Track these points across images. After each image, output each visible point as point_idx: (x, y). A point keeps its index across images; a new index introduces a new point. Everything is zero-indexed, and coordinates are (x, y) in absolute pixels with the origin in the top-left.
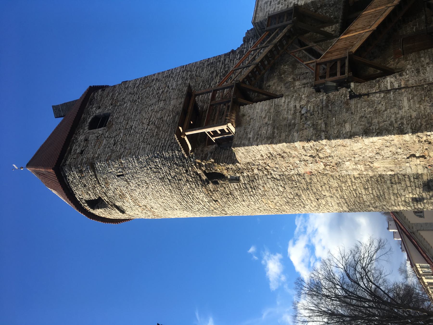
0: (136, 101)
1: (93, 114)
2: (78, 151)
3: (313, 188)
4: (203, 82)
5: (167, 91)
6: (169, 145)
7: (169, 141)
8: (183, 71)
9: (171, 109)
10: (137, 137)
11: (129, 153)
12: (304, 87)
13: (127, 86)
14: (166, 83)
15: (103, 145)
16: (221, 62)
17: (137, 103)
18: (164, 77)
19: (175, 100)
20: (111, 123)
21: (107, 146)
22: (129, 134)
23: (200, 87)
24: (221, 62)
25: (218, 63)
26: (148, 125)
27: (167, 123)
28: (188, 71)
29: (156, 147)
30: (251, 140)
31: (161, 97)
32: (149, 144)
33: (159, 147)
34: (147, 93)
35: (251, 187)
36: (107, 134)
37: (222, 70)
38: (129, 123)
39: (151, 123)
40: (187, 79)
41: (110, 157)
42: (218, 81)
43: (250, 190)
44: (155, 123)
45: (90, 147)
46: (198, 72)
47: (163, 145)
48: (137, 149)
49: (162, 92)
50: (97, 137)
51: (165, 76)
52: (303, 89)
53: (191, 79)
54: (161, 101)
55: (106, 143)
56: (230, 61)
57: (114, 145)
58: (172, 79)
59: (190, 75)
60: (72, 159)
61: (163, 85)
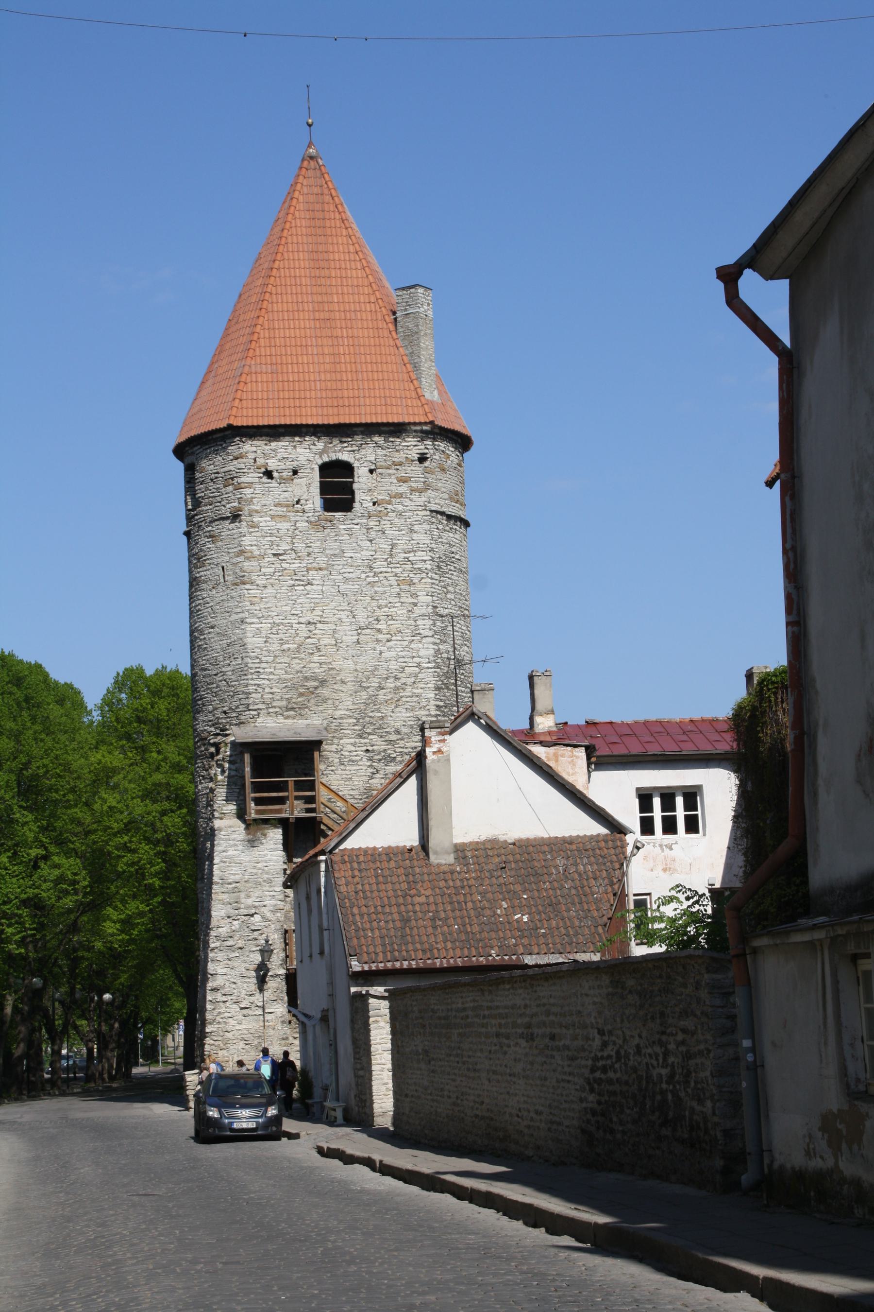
4: (383, 717)
5: (378, 641)
6: (259, 685)
7: (267, 682)
8: (418, 665)
10: (284, 608)
11: (254, 599)
13: (416, 528)
14: (400, 632)
17: (363, 575)
18: (415, 621)
19: (353, 667)
22: (294, 585)
23: (371, 714)
27: (304, 667)
28: (416, 676)
29: (258, 658)
32: (265, 642)
34: (385, 592)
39: (312, 627)
40: (396, 678)
41: (248, 558)
42: (375, 748)
44: (309, 637)
45: (277, 492)
46: (408, 699)
47: (261, 670)
48: (260, 615)
49: (379, 631)
50: (298, 502)
53: (397, 689)
61: (396, 625)
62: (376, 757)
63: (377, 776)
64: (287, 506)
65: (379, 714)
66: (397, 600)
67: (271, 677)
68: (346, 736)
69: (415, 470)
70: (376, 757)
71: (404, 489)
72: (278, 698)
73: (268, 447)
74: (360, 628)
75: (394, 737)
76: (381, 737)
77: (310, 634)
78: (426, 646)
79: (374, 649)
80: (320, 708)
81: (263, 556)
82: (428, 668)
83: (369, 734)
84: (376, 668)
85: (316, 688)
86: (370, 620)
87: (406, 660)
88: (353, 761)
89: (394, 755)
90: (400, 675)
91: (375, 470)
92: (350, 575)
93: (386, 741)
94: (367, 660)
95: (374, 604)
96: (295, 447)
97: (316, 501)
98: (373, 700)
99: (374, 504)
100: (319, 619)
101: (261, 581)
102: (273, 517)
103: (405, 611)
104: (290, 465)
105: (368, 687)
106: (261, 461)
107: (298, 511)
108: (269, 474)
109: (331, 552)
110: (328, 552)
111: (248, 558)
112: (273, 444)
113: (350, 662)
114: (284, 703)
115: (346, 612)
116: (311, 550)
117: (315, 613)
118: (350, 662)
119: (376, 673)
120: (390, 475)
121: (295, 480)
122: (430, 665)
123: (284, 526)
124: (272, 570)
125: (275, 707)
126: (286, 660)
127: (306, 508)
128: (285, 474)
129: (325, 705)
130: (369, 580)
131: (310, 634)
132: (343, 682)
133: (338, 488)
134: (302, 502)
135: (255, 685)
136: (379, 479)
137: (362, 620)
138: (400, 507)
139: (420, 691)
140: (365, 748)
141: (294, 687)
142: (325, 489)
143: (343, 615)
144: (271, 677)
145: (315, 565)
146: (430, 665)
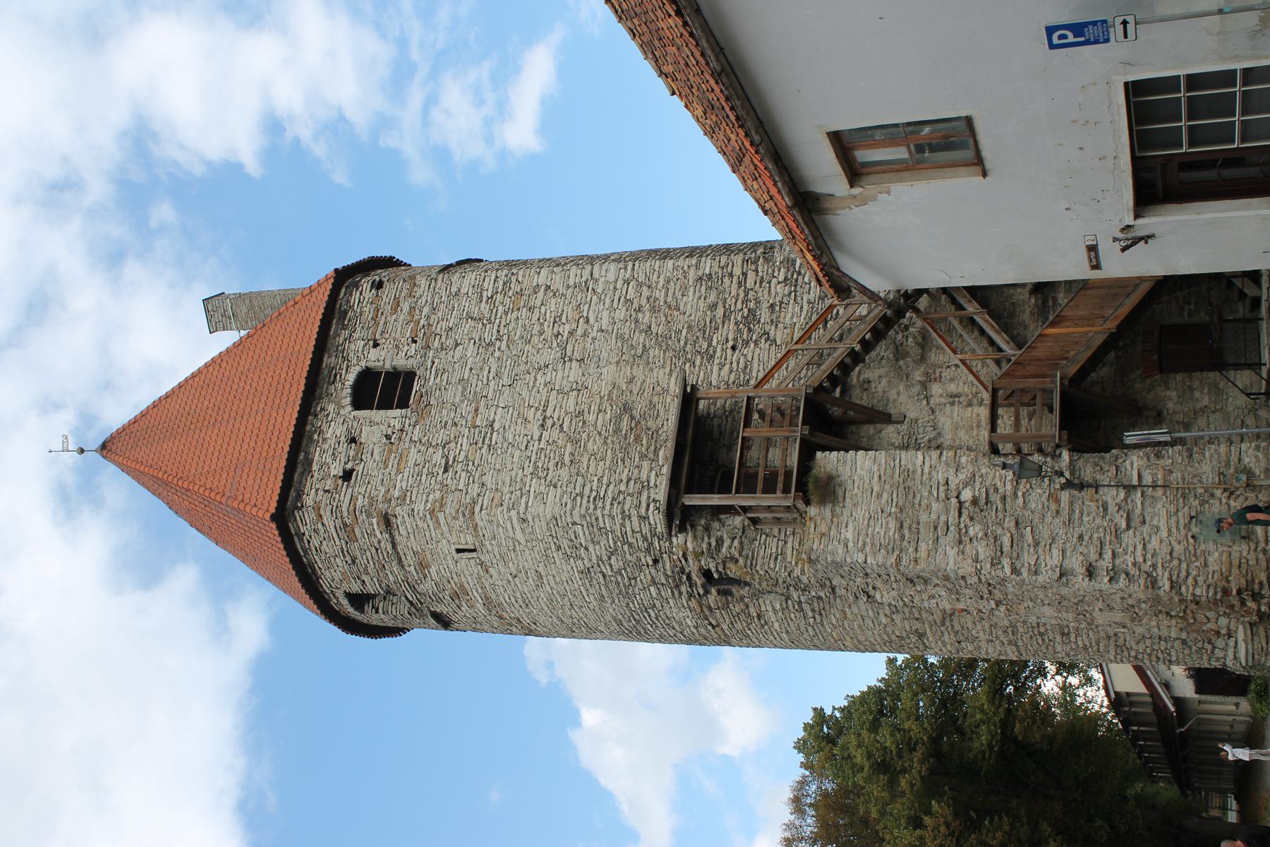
0: (490, 344)
1: (359, 359)
2: (333, 472)
3: (956, 624)
4: (689, 327)
5: (585, 335)
6: (614, 499)
7: (612, 487)
8: (627, 282)
9: (605, 392)
11: (496, 501)
12: (952, 404)
13: (454, 289)
15: (411, 463)
16: (735, 279)
17: (497, 354)
18: (568, 287)
19: (613, 367)
20: (424, 398)
21: (425, 470)
22: (489, 446)
23: (682, 343)
24: (735, 279)
25: (726, 280)
26: (542, 426)
27: (600, 434)
28: (641, 285)
29: (575, 499)
30: (851, 544)
31: (569, 348)
32: (555, 487)
33: (585, 499)
35: (813, 610)
36: (416, 432)
37: (739, 305)
38: (481, 409)
39: (549, 422)
40: (639, 310)
42: (731, 337)
43: (810, 614)
44: (561, 426)
45: (370, 464)
46: (670, 294)
47: (594, 494)
48: (518, 493)
49: (571, 333)
50: (388, 437)
51: (571, 283)
52: (948, 407)
53: (654, 310)
54: (571, 360)
55: (420, 460)
56: (761, 283)
57: (446, 470)
58: (595, 298)
59: (648, 299)
60: (320, 493)
61: (570, 312)
62: (745, 337)
63: (772, 333)
64: (390, 451)
65: (685, 331)
66: (537, 310)
67: (605, 481)
68: (708, 375)
69: (388, 292)
70: (745, 337)
71: (405, 307)
72: (636, 471)
73: (316, 475)
74: (563, 358)
75: (720, 312)
76: (717, 329)
77: (557, 426)
78: (603, 273)
79: (594, 339)
80: (662, 413)
81: (444, 485)
82: (633, 269)
83: (710, 345)
84: (620, 337)
85: (632, 418)
86: (555, 345)
87: (616, 298)
88: (746, 367)
89: (746, 311)
90: (636, 305)
91: (375, 340)
92: (493, 370)
93: (723, 323)
94: (607, 348)
95: (535, 339)
96: (325, 440)
97: (393, 416)
98: (662, 341)
99: (415, 342)
100: (539, 413)
101: (474, 490)
102: (399, 472)
103: (553, 301)
104: (343, 448)
105: (644, 346)
106: (329, 484)
107: (400, 439)
108: (347, 475)
109: (459, 395)
110: (457, 400)
111: (442, 506)
112: (315, 467)
113: (605, 371)
114: (646, 464)
115: (539, 377)
116: (450, 422)
117: (531, 417)
118: (605, 371)
119: (627, 336)
120: (385, 323)
121: (362, 440)
122: (629, 268)
123: (414, 456)
124: (464, 474)
125: (648, 477)
126: (585, 460)
127: (398, 426)
128: (352, 453)
129: (659, 407)
130: (503, 347)
131: (557, 426)
132: (631, 381)
133: (384, 389)
134: (390, 432)
135: (612, 504)
136: (387, 336)
137: (550, 355)
138: (426, 310)
139: (661, 279)
140: (729, 352)
141: (625, 451)
142: (385, 405)
143: (541, 380)
144: (605, 481)
145: (470, 418)
146: (629, 268)
